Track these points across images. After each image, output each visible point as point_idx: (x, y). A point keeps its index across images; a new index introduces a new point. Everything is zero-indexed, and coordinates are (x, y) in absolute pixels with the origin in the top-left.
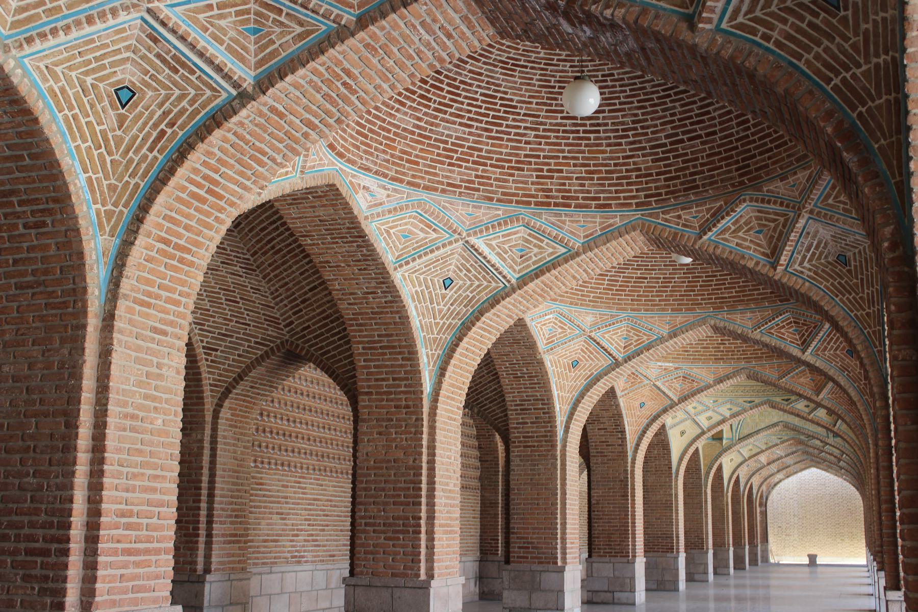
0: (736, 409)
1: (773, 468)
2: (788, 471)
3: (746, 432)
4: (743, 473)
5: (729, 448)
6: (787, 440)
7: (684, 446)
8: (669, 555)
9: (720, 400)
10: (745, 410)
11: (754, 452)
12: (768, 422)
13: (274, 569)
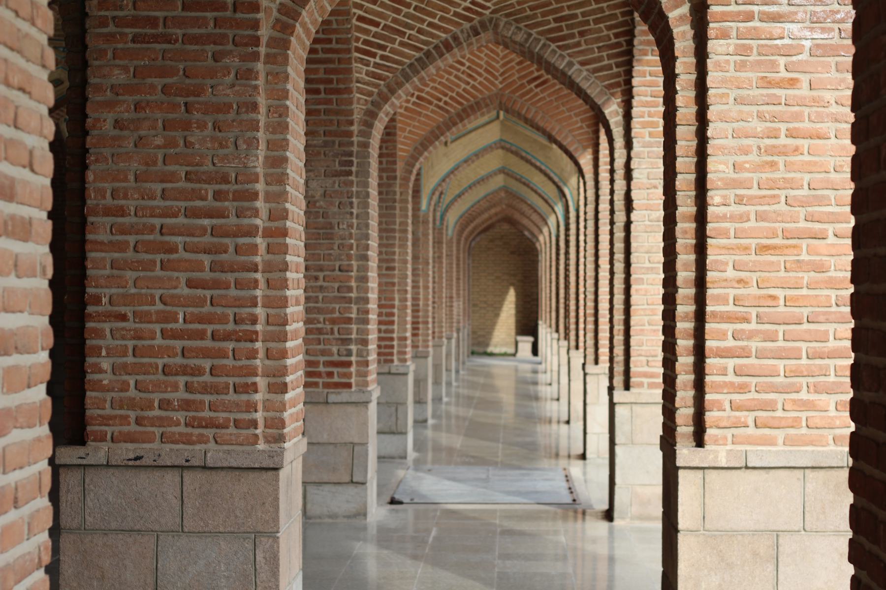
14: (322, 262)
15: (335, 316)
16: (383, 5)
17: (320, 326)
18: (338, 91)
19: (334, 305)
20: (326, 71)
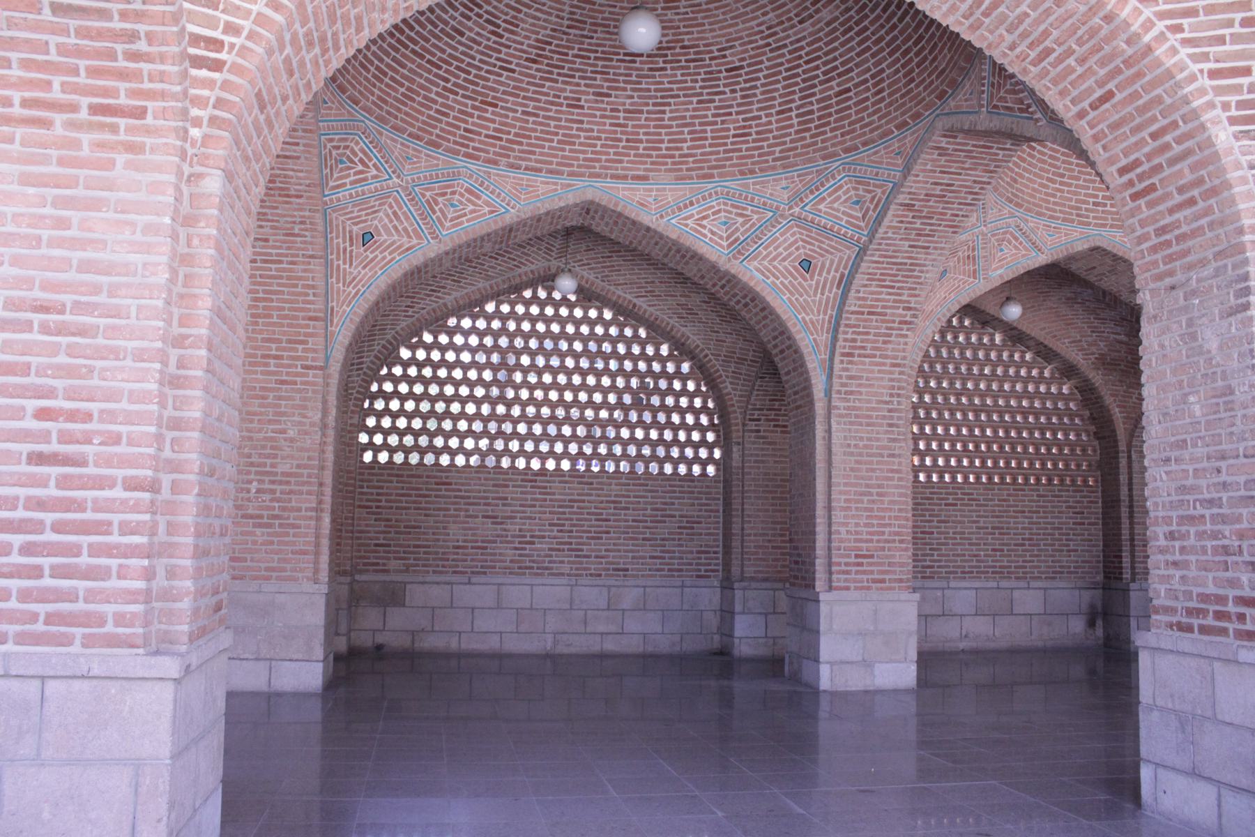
13: (474, 580)
14: (1224, 447)
15: (1243, 526)
16: (507, 5)
17: (1226, 542)
18: (1214, 192)
19: (1240, 510)
20: (1193, 168)
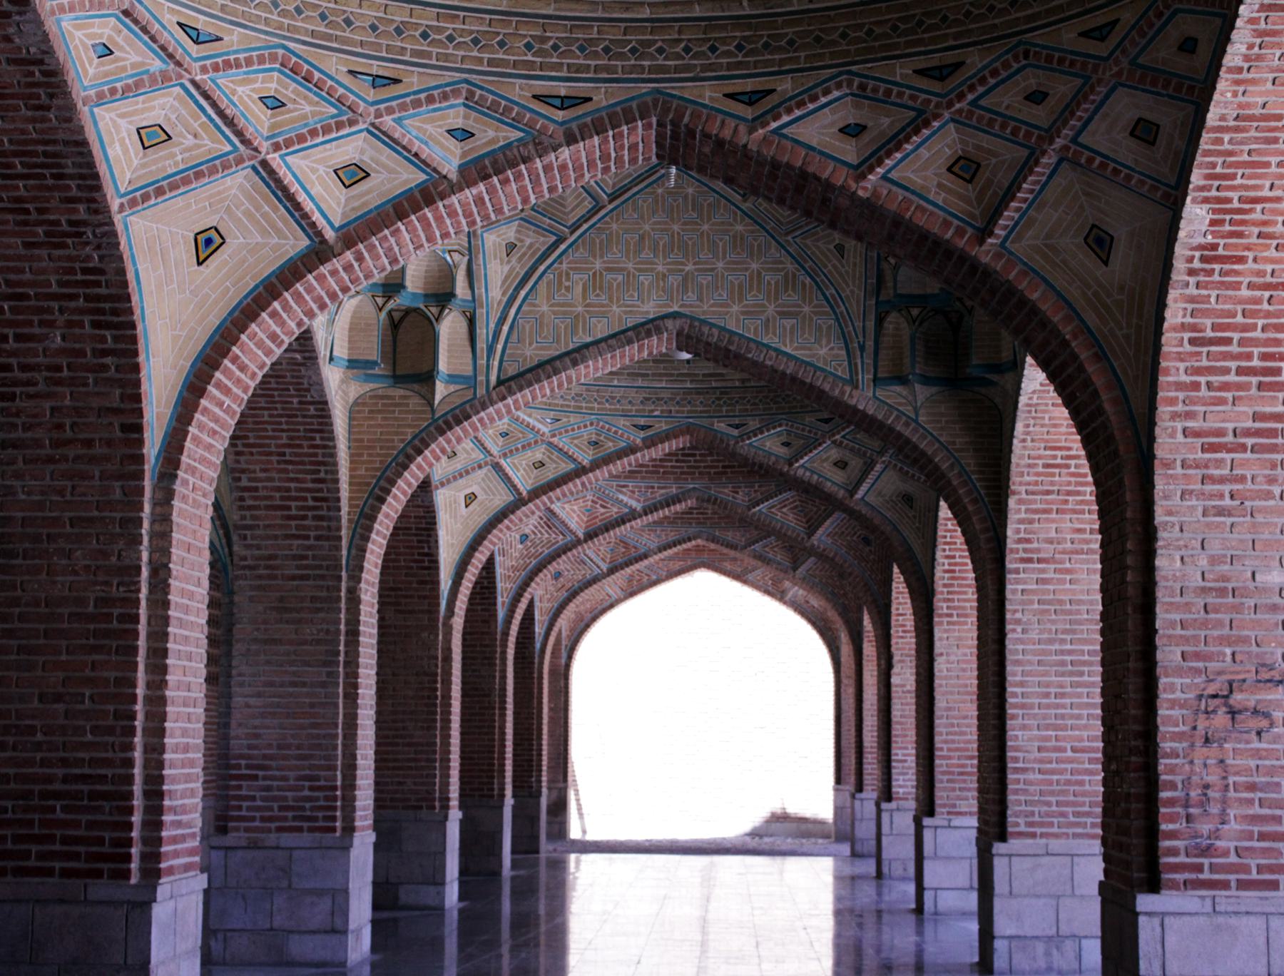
0: (491, 135)
1: (597, 553)
2: (636, 572)
3: (532, 353)
4: (508, 550)
5: (459, 416)
6: (666, 436)
7: (214, 320)
8: (101, 889)
9: (414, 80)
10: (541, 145)
11: (550, 473)
12: (619, 315)
